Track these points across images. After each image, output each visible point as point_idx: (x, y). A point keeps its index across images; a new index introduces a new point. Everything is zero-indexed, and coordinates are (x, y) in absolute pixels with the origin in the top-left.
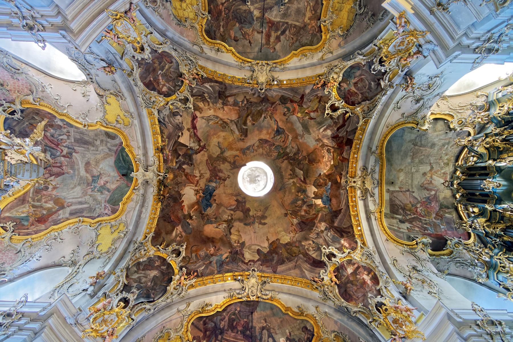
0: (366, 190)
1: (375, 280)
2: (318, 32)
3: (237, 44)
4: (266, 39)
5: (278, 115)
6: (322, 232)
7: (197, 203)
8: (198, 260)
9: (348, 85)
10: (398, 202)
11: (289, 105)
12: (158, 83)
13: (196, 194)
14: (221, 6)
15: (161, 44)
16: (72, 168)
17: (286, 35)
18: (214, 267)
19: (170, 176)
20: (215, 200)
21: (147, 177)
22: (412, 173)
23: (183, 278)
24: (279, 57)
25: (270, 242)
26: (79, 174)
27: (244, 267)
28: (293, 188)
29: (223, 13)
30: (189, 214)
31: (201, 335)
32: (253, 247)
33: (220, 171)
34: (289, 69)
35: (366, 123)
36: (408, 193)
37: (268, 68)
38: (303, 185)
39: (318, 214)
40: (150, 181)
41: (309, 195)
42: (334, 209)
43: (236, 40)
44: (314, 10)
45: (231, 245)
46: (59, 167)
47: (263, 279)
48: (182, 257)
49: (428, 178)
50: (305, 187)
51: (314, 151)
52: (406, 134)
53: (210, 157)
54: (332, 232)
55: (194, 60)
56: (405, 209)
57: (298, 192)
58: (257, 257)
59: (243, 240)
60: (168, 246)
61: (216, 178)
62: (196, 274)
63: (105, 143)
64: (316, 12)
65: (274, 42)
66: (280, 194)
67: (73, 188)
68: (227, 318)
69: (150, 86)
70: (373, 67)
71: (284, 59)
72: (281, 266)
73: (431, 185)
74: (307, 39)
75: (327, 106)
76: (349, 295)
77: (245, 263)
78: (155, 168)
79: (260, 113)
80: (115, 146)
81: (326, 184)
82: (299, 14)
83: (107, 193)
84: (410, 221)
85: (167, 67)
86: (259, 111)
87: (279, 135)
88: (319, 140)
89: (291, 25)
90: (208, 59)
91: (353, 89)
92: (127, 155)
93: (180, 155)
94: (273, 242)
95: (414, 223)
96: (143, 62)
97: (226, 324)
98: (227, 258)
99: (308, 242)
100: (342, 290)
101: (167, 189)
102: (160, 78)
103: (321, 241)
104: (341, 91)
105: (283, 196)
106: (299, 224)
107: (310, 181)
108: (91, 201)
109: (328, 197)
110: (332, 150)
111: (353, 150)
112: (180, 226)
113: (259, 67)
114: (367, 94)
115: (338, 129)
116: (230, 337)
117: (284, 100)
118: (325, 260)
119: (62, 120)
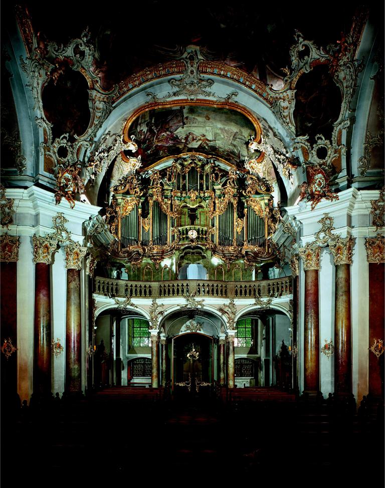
36: (182, 124)
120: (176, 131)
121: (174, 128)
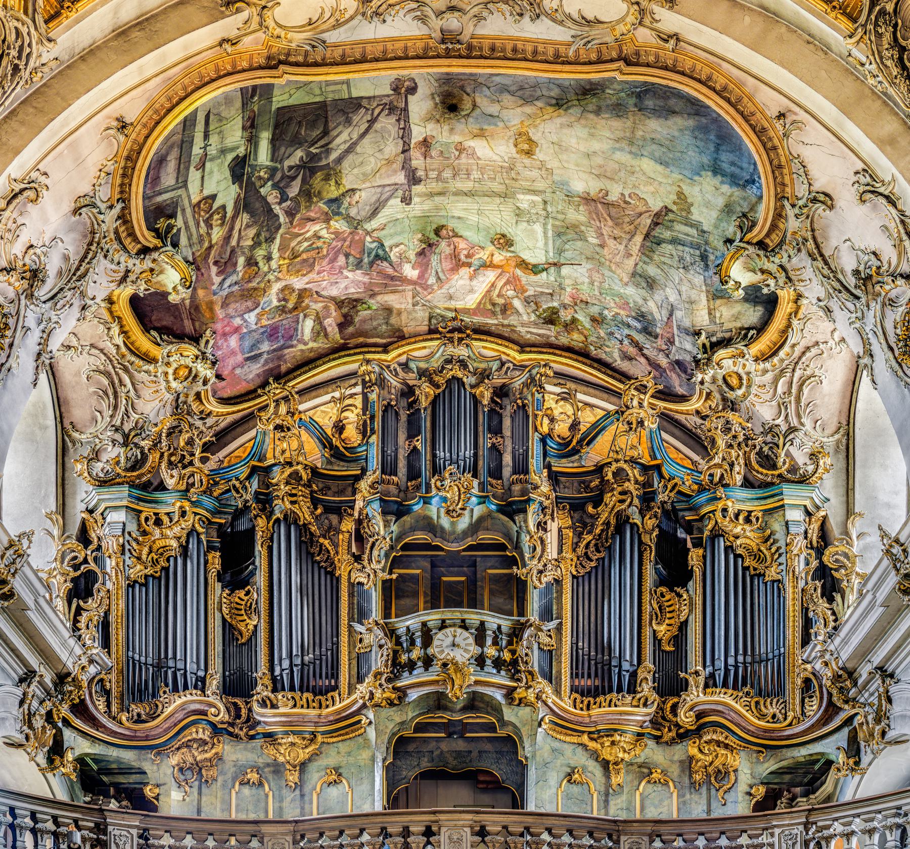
22: (505, 196)
36: (401, 178)
49: (484, 255)
73: (447, 265)
95: (245, 218)
120: (375, 213)
121: (365, 197)
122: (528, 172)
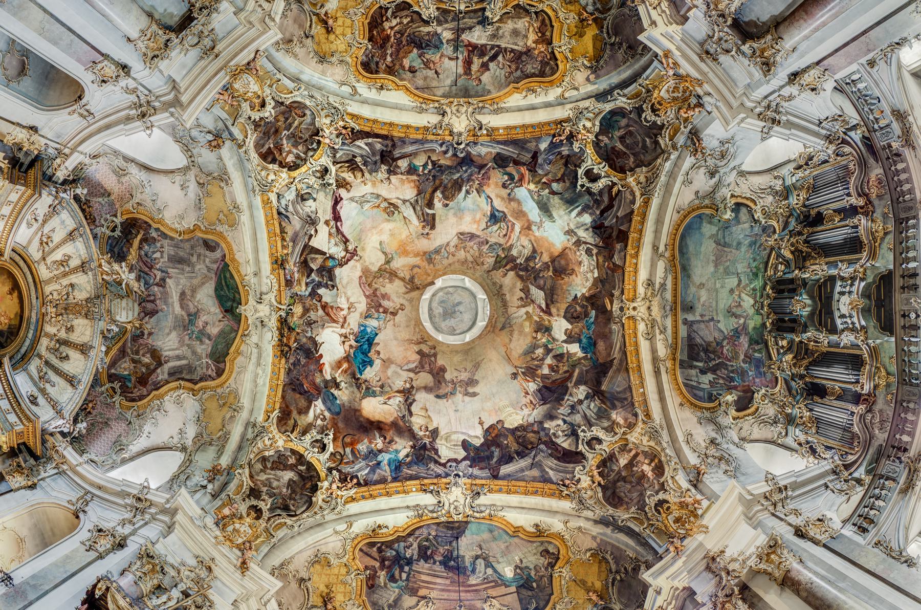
0: (653, 323)
1: (659, 470)
2: (551, 59)
3: (414, 77)
4: (464, 67)
5: (492, 186)
6: (580, 402)
7: (347, 358)
8: (357, 458)
9: (611, 139)
10: (699, 340)
11: (511, 169)
12: (280, 151)
13: (344, 342)
14: (389, 31)
15: (292, 92)
16: (166, 303)
17: (499, 62)
18: (386, 471)
19: (298, 310)
20: (378, 353)
21: (261, 314)
22: (717, 291)
23: (334, 486)
24: (489, 92)
25: (486, 426)
26: (173, 311)
27: (440, 470)
28: (527, 324)
29: (392, 39)
30: (334, 380)
31: (377, 565)
32: (454, 437)
33: (385, 296)
34: (508, 110)
35: (647, 203)
36: (712, 323)
37: (470, 110)
38: (546, 317)
39: (573, 372)
40: (266, 320)
41: (557, 336)
42: (601, 361)
43: (412, 70)
44: (540, 32)
45: (413, 435)
46: (153, 302)
47: (474, 488)
48: (329, 453)
49: (736, 297)
50: (549, 321)
51: (563, 254)
52: (704, 224)
53: (366, 272)
54: (598, 402)
55: (340, 108)
56: (707, 350)
57: (536, 332)
58: (462, 454)
59: (435, 425)
60: (304, 433)
61: (378, 311)
62: (355, 481)
63: (202, 258)
64: (543, 34)
65: (478, 71)
66: (503, 337)
67: (168, 334)
68: (415, 545)
69: (268, 156)
70: (644, 116)
71: (498, 94)
72: (507, 466)
73: (740, 309)
74: (533, 68)
75: (580, 172)
76: (619, 498)
77: (440, 464)
78: (272, 297)
79: (458, 186)
80: (215, 262)
81: (587, 315)
82: (517, 36)
83: (207, 341)
84: (713, 370)
85: (296, 123)
86: (456, 181)
87: (495, 224)
88: (570, 232)
89: (506, 49)
90: (365, 102)
91: (619, 146)
92: (232, 276)
93: (312, 270)
94: (492, 427)
95: (718, 372)
96: (262, 123)
97: (416, 553)
98: (407, 456)
99: (554, 423)
100: (609, 493)
101: (293, 335)
102: (285, 142)
103: (578, 418)
104: (601, 148)
105: (507, 341)
106: (539, 391)
107: (558, 310)
108: (189, 354)
109: (590, 337)
110: (595, 251)
111: (630, 251)
112: (320, 400)
113: (454, 109)
114: (642, 157)
115: (602, 213)
116: (423, 568)
117: (501, 161)
118: (584, 451)
119: (157, 230)
120: (722, 332)
121: (717, 335)
122: (710, 285)
